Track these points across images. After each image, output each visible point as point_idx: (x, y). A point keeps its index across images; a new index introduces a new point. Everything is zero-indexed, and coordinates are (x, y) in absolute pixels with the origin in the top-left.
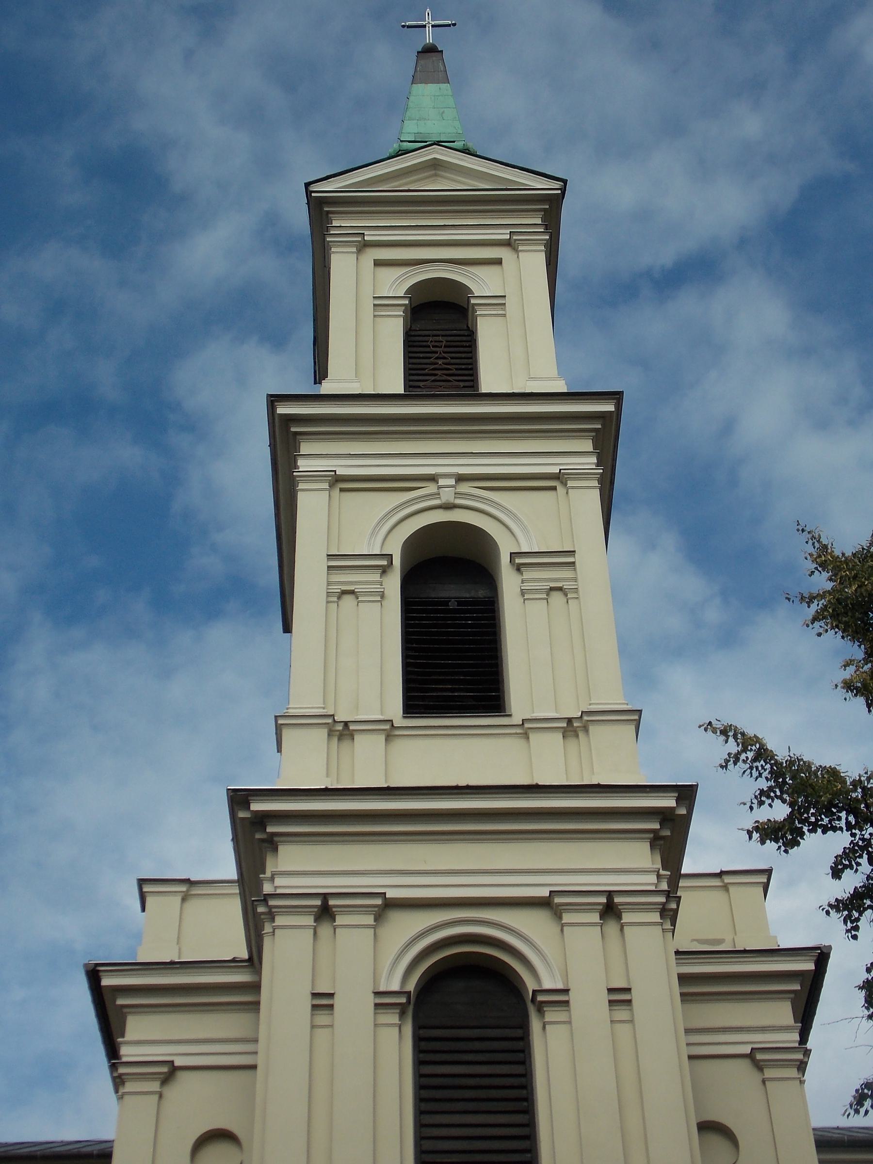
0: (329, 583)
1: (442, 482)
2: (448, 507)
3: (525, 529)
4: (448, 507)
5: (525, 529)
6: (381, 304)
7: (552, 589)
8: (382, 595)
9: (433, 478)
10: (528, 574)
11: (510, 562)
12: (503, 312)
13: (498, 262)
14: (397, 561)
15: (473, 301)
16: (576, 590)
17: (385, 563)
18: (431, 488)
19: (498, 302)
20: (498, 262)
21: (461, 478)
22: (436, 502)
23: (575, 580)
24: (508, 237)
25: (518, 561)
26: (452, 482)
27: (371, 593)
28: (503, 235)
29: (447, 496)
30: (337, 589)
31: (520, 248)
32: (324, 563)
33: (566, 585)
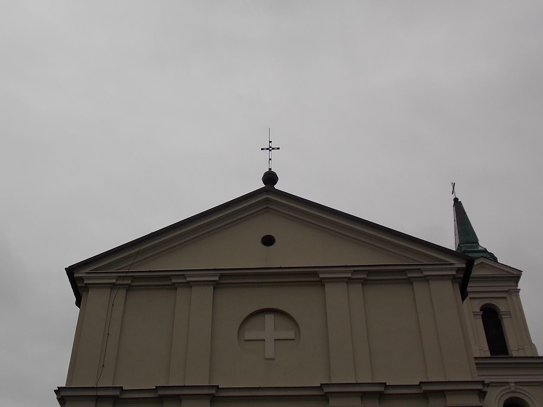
1: (511, 385)
2: (514, 392)
4: (514, 392)
6: (475, 314)
9: (508, 383)
12: (510, 317)
13: (505, 298)
15: (501, 313)
18: (507, 387)
19: (509, 314)
20: (505, 298)
21: (516, 383)
22: (509, 391)
24: (508, 290)
26: (513, 384)
28: (506, 289)
29: (513, 389)
31: (512, 294)
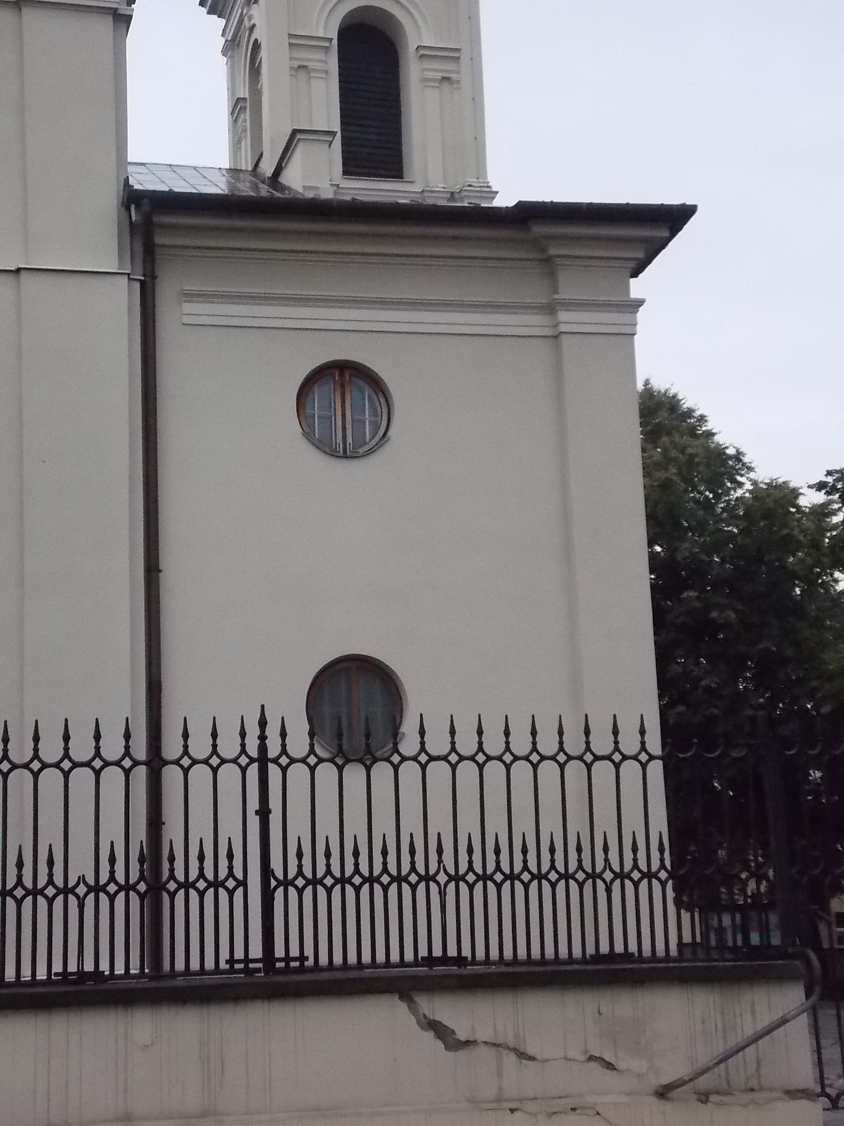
0: (291, 59)
3: (420, 12)
5: (420, 12)
7: (444, 78)
8: (327, 72)
10: (427, 64)
11: (417, 49)
14: (335, 42)
16: (458, 82)
17: (327, 44)
23: (458, 72)
25: (422, 52)
27: (319, 71)
30: (296, 64)
32: (286, 41)
33: (454, 76)
